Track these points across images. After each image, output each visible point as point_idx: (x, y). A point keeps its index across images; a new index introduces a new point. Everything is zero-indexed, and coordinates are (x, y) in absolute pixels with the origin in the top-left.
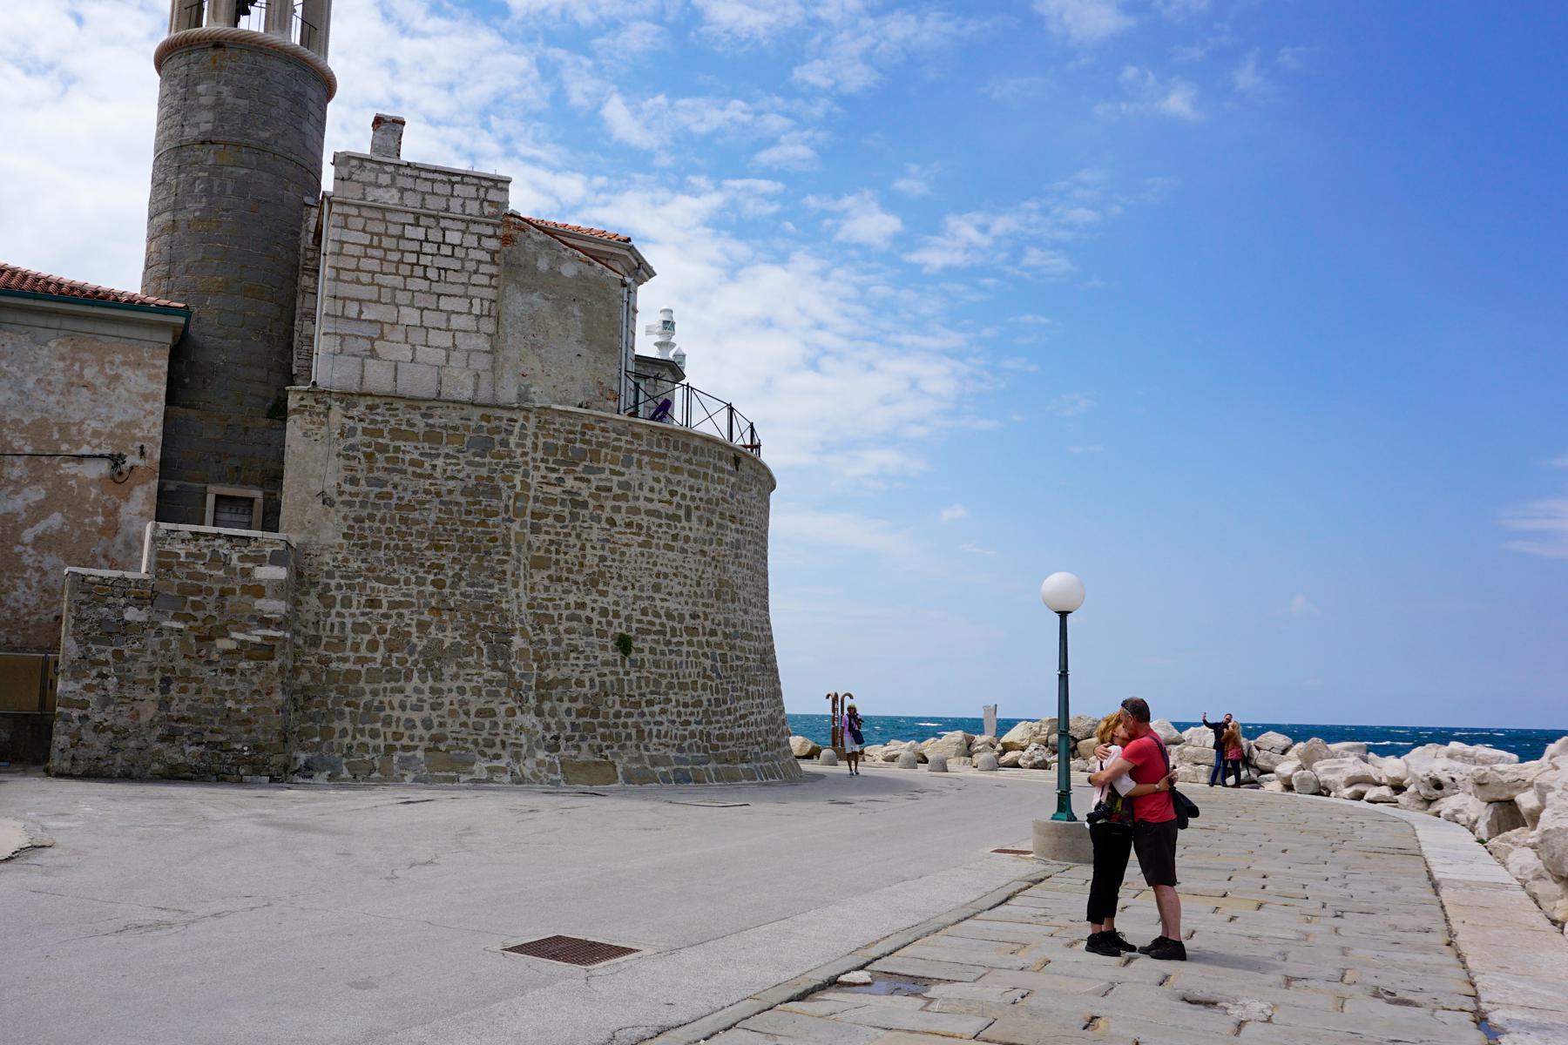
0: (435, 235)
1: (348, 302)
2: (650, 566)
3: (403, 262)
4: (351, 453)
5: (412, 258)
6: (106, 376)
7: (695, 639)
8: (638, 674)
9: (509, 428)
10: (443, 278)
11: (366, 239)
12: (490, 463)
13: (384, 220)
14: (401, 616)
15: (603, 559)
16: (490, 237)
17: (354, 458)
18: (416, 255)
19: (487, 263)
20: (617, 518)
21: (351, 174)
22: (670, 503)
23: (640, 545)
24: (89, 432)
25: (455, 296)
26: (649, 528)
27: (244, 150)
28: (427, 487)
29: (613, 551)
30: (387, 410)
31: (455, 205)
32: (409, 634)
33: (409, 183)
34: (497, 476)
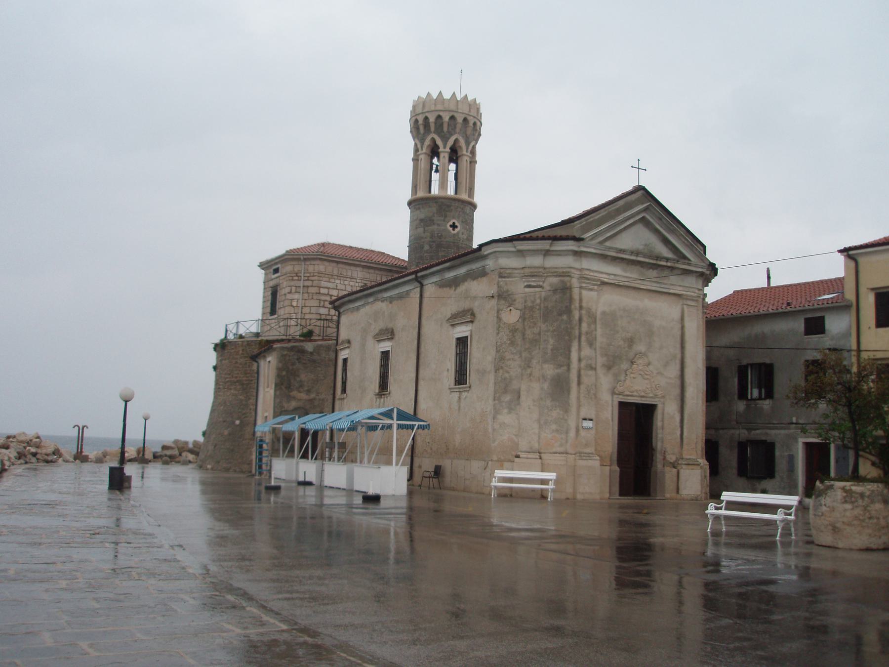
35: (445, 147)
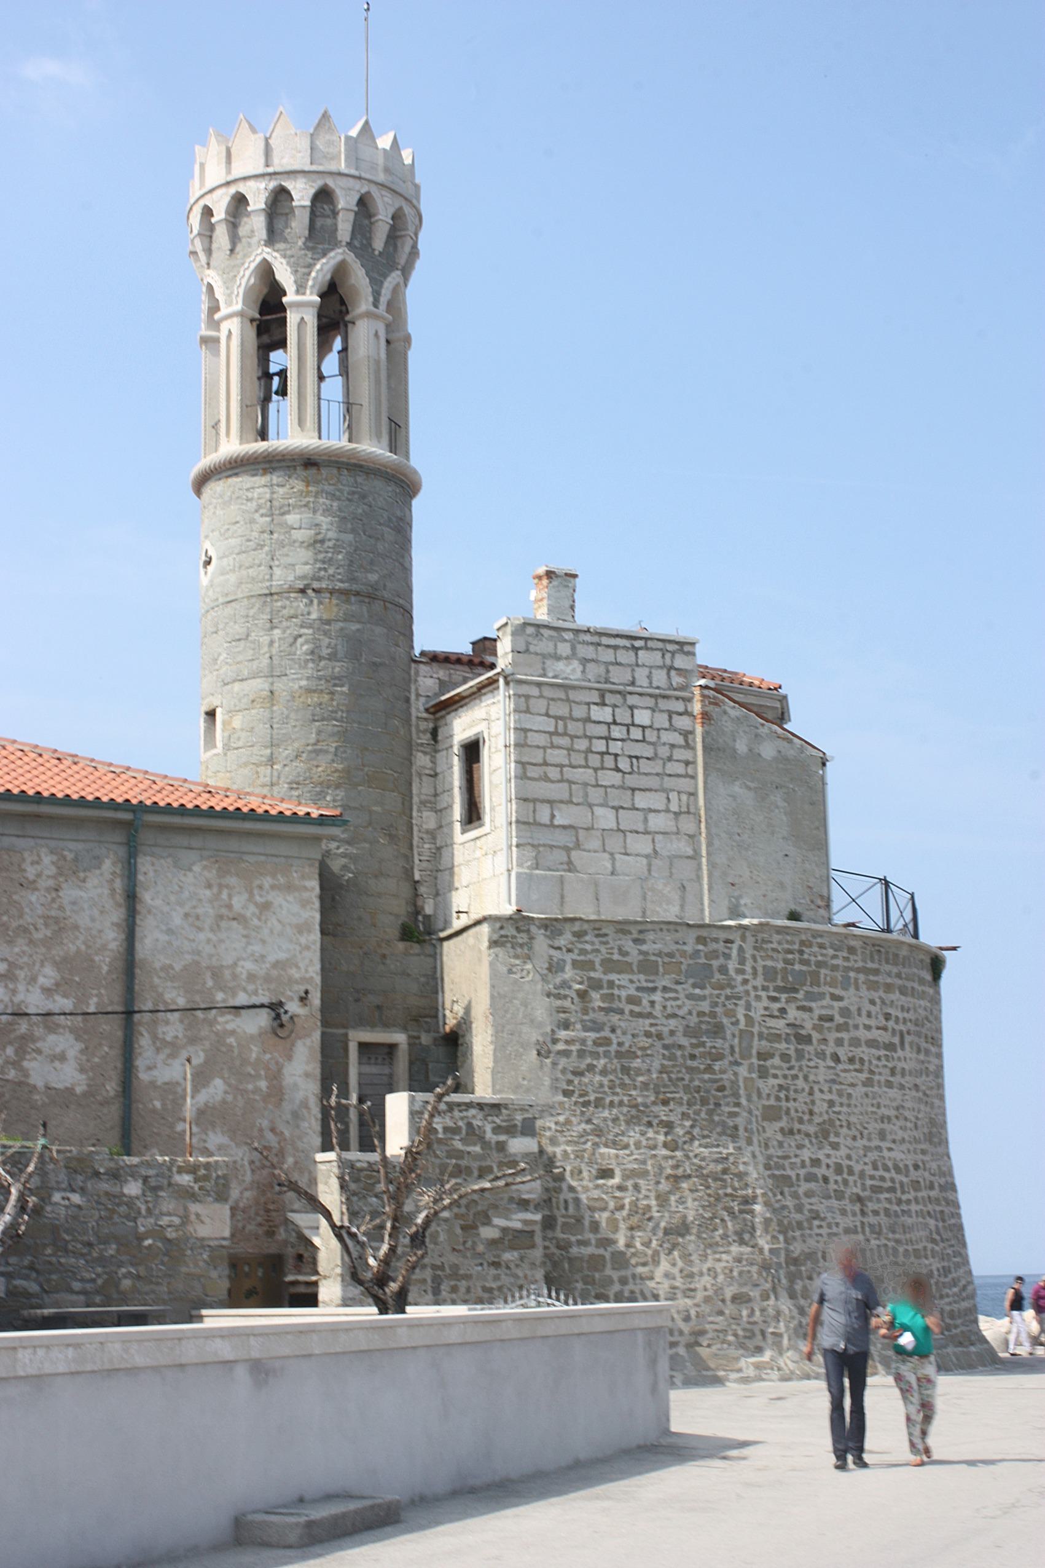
0: (623, 716)
1: (538, 805)
2: (874, 1109)
3: (592, 752)
4: (562, 992)
5: (600, 746)
6: (256, 904)
7: (920, 1194)
8: (877, 1242)
9: (727, 951)
10: (635, 769)
11: (549, 725)
12: (711, 995)
13: (568, 700)
14: (636, 1187)
15: (831, 1103)
16: (680, 714)
17: (565, 997)
18: (604, 742)
19: (680, 747)
20: (842, 1053)
21: (528, 644)
22: (885, 1029)
23: (864, 1084)
24: (244, 976)
25: (650, 790)
26: (870, 1062)
27: (353, 599)
28: (647, 1028)
29: (840, 1093)
30: (597, 936)
31: (641, 675)
32: (649, 1207)
33: (589, 652)
34: (719, 1010)
35: (300, 289)
